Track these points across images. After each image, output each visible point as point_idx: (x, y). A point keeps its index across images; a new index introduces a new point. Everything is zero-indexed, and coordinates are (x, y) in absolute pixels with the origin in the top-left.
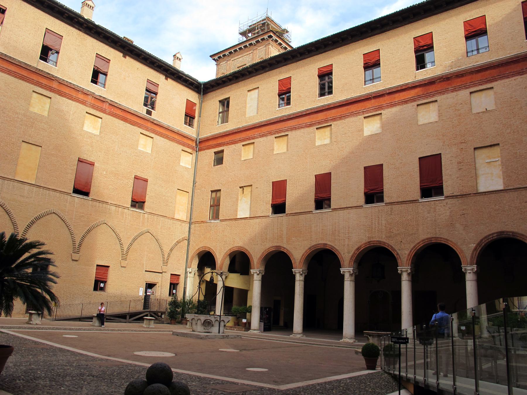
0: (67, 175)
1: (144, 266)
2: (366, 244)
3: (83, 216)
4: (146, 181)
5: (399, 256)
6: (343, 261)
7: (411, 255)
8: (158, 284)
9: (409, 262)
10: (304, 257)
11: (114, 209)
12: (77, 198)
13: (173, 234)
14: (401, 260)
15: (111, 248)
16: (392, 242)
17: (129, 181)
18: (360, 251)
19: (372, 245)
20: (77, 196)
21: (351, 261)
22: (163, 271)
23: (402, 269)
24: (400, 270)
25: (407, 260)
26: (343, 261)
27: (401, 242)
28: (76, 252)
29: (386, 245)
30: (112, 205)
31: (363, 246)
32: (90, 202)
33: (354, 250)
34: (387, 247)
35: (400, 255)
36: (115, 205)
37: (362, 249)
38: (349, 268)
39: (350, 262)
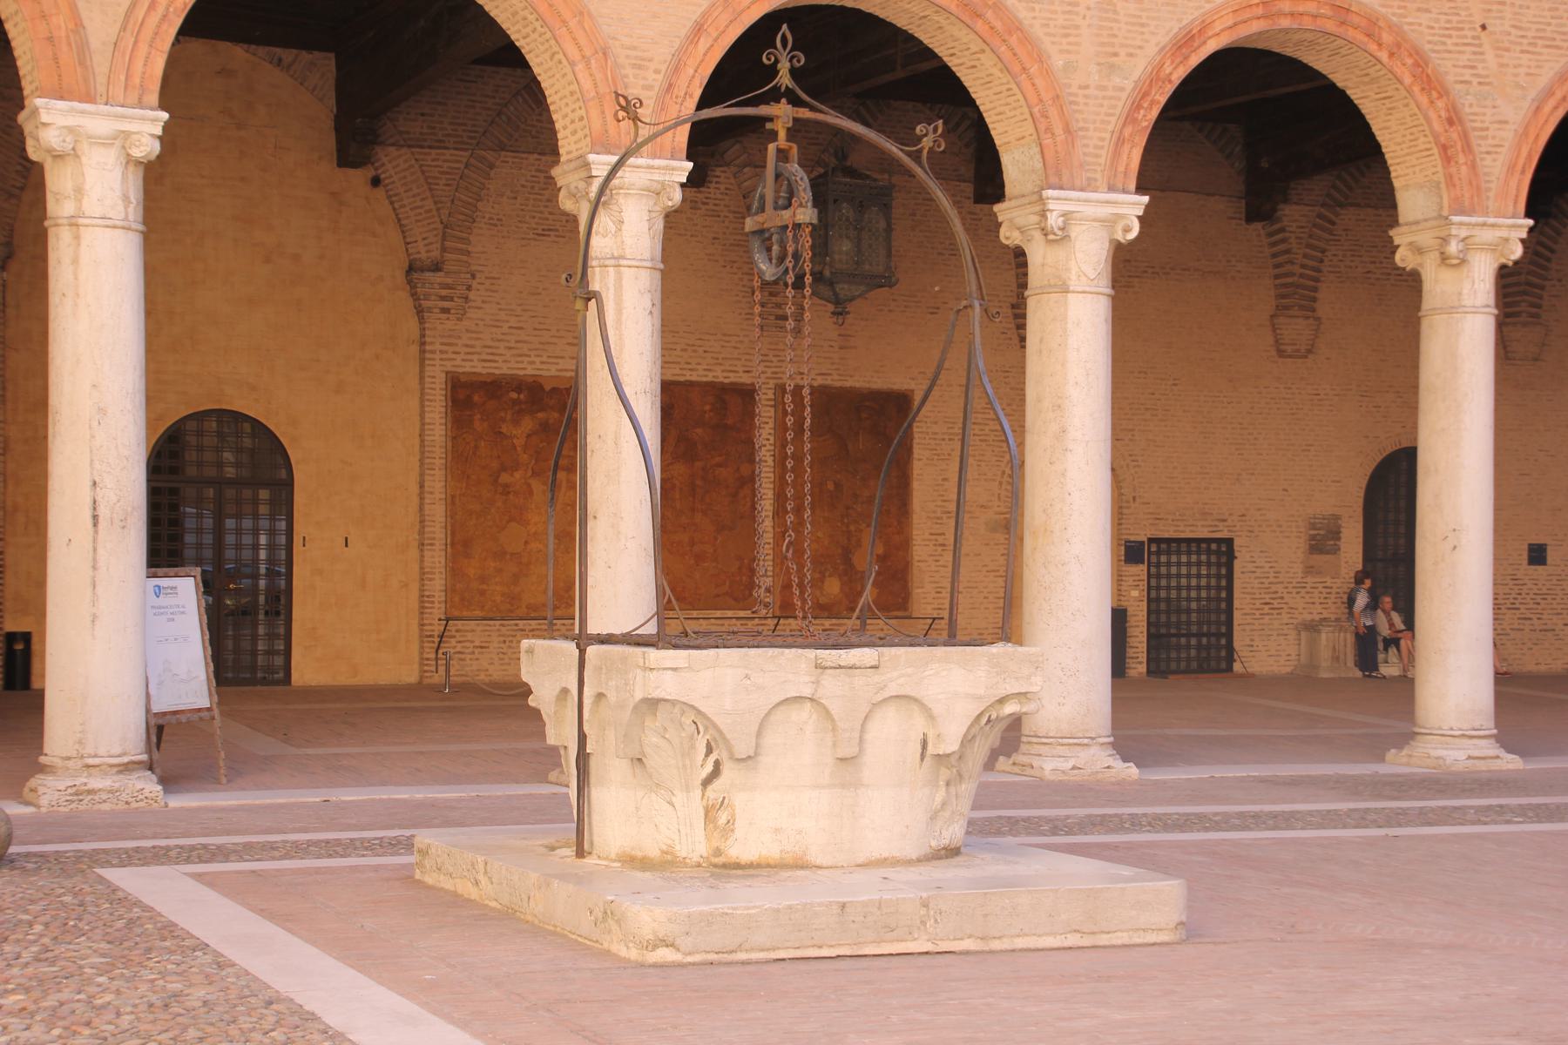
2: (1247, 15)
5: (1465, 136)
6: (1067, 130)
7: (1537, 136)
9: (1520, 181)
10: (703, 45)
14: (1473, 166)
16: (1424, 19)
18: (1195, 60)
19: (1285, 23)
21: (1127, 131)
23: (1476, 232)
24: (1463, 233)
25: (1511, 169)
26: (1067, 130)
27: (1484, 27)
29: (1386, 38)
31: (1218, 27)
33: (1151, 50)
34: (1384, 56)
35: (1469, 125)
37: (1212, 46)
38: (1111, 188)
39: (1120, 142)
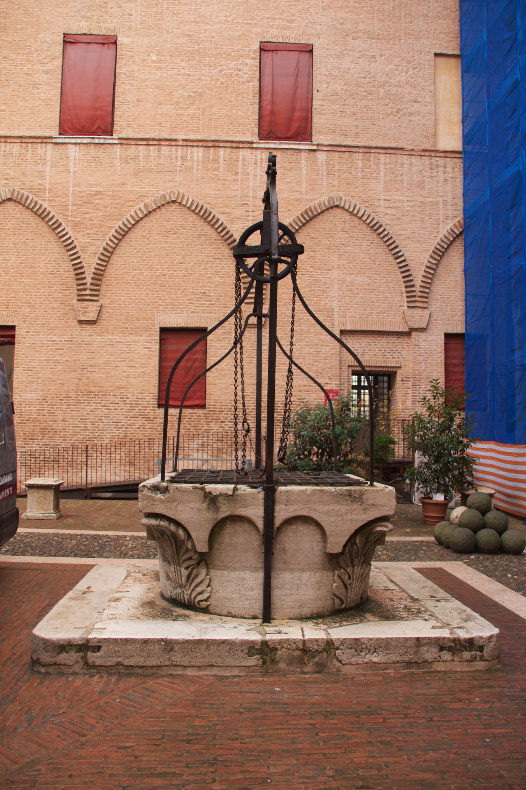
0: (35, 91)
1: (336, 316)
3: (98, 193)
4: (309, 50)
8: (399, 372)
11: (201, 155)
12: (74, 146)
13: (437, 204)
15: (203, 272)
17: (243, 63)
20: (73, 141)
22: (411, 324)
28: (88, 298)
30: (189, 143)
32: (118, 149)
36: (201, 144)
